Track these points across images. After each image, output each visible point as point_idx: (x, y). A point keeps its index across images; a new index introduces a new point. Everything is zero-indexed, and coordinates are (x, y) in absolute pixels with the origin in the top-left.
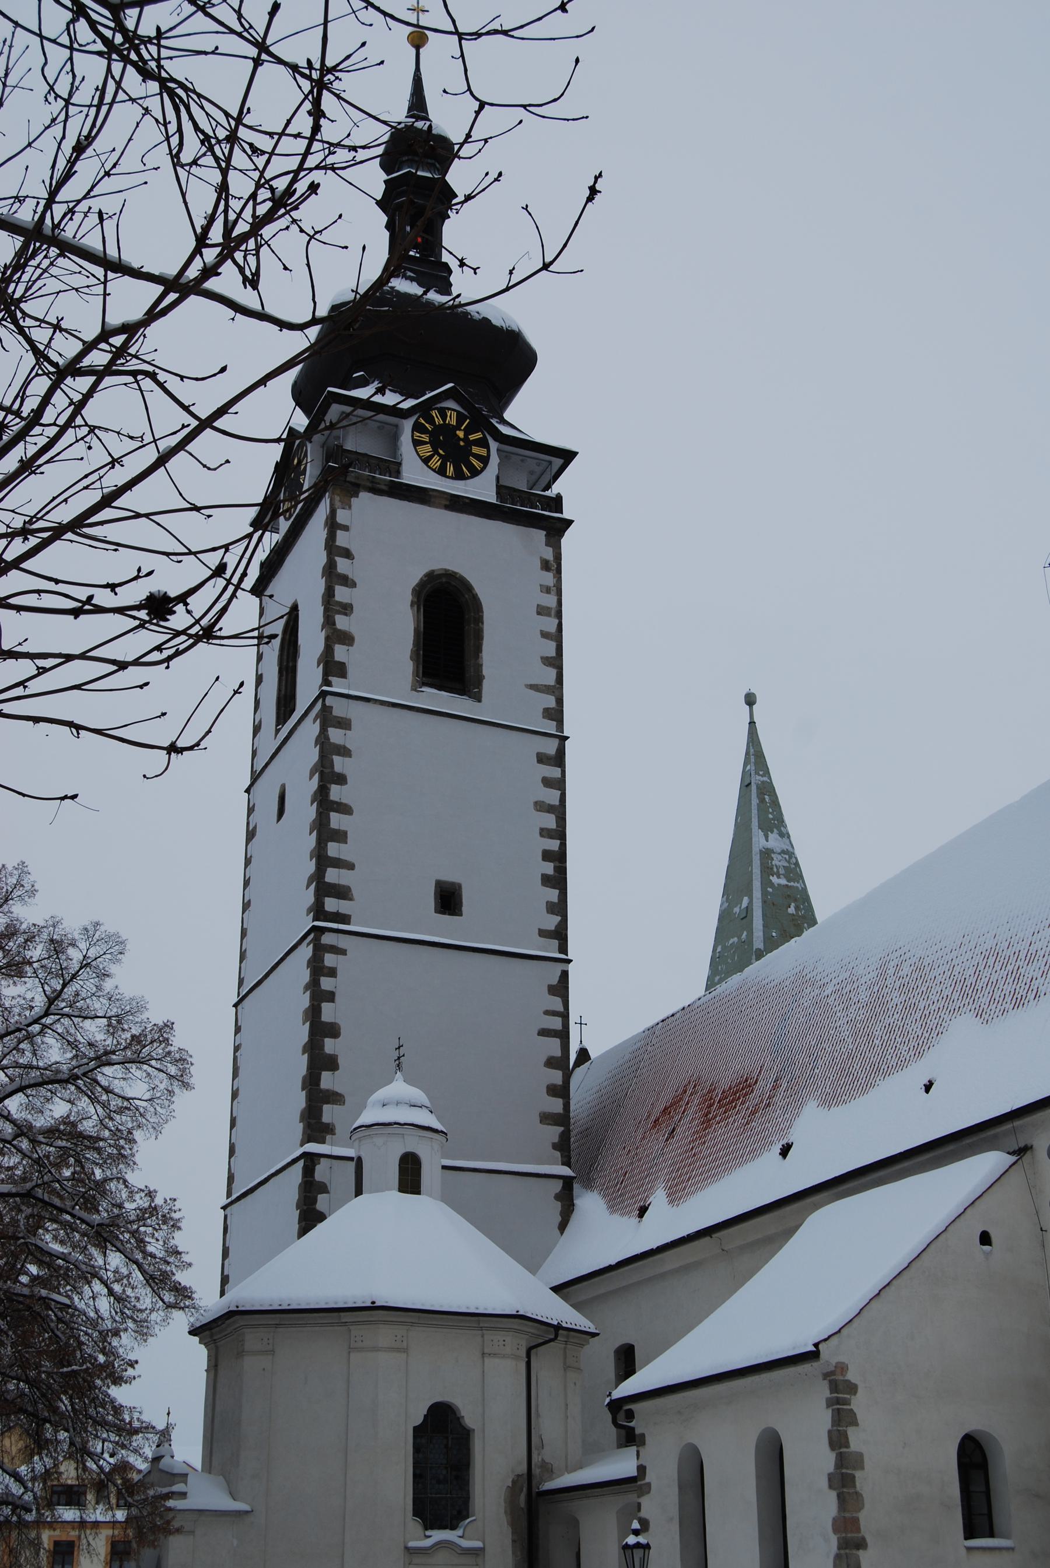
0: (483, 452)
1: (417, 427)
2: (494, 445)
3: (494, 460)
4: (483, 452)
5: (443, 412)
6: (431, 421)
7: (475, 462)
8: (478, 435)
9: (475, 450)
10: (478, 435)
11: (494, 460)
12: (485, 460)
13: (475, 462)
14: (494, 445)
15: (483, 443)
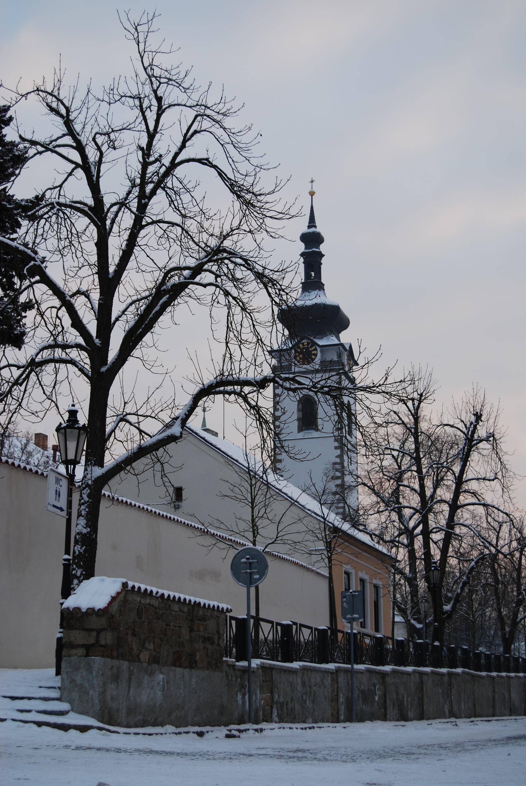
0: (315, 352)
1: (296, 352)
2: (318, 349)
3: (319, 354)
4: (315, 352)
5: (303, 344)
6: (299, 348)
7: (313, 357)
8: (314, 347)
9: (313, 352)
10: (314, 347)
11: (319, 354)
12: (316, 355)
13: (313, 357)
14: (318, 349)
15: (316, 349)
